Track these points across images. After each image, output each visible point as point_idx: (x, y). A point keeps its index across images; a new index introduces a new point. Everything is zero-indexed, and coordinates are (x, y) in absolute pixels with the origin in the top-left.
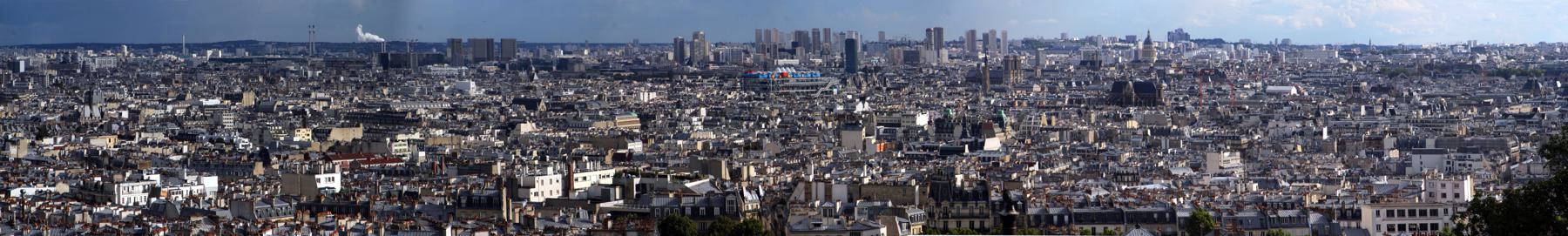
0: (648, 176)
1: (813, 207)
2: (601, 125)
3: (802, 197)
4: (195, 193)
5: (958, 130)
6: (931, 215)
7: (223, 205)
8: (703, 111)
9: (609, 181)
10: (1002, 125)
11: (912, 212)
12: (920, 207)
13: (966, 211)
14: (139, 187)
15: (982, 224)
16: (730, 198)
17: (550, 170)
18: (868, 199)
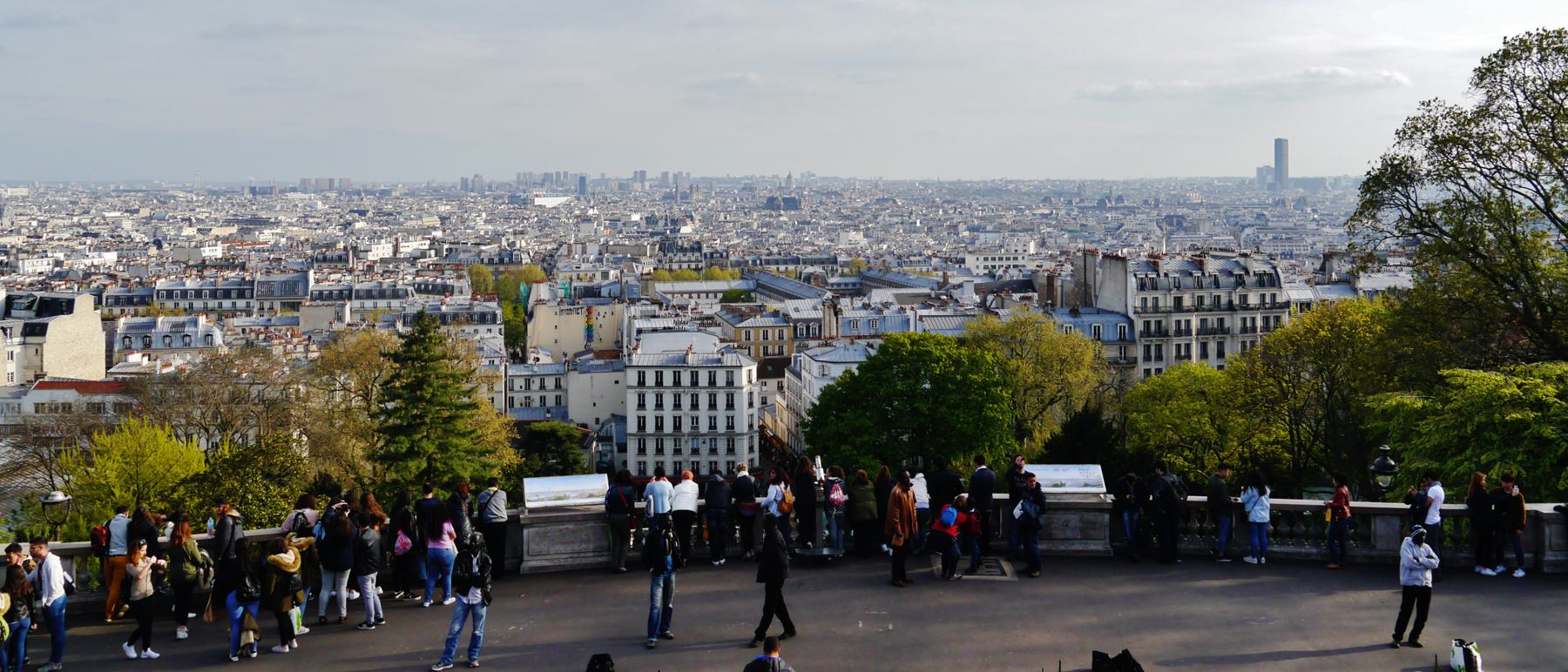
0: (454, 243)
1: (573, 258)
2: (414, 223)
3: (566, 253)
4: (96, 263)
5: (661, 223)
6: (660, 261)
7: (121, 269)
8: (484, 215)
9: (427, 247)
10: (692, 220)
11: (643, 260)
12: (651, 257)
13: (686, 259)
14: (45, 261)
15: (697, 266)
16: (515, 253)
17: (383, 241)
18: (613, 253)
